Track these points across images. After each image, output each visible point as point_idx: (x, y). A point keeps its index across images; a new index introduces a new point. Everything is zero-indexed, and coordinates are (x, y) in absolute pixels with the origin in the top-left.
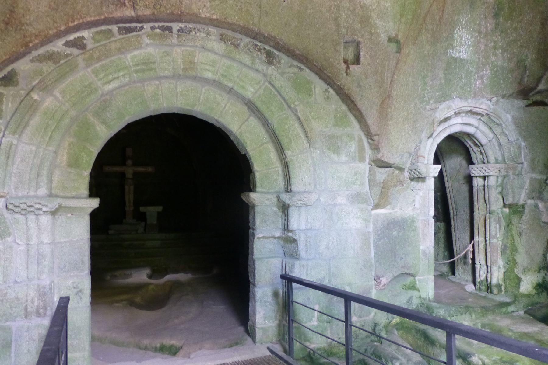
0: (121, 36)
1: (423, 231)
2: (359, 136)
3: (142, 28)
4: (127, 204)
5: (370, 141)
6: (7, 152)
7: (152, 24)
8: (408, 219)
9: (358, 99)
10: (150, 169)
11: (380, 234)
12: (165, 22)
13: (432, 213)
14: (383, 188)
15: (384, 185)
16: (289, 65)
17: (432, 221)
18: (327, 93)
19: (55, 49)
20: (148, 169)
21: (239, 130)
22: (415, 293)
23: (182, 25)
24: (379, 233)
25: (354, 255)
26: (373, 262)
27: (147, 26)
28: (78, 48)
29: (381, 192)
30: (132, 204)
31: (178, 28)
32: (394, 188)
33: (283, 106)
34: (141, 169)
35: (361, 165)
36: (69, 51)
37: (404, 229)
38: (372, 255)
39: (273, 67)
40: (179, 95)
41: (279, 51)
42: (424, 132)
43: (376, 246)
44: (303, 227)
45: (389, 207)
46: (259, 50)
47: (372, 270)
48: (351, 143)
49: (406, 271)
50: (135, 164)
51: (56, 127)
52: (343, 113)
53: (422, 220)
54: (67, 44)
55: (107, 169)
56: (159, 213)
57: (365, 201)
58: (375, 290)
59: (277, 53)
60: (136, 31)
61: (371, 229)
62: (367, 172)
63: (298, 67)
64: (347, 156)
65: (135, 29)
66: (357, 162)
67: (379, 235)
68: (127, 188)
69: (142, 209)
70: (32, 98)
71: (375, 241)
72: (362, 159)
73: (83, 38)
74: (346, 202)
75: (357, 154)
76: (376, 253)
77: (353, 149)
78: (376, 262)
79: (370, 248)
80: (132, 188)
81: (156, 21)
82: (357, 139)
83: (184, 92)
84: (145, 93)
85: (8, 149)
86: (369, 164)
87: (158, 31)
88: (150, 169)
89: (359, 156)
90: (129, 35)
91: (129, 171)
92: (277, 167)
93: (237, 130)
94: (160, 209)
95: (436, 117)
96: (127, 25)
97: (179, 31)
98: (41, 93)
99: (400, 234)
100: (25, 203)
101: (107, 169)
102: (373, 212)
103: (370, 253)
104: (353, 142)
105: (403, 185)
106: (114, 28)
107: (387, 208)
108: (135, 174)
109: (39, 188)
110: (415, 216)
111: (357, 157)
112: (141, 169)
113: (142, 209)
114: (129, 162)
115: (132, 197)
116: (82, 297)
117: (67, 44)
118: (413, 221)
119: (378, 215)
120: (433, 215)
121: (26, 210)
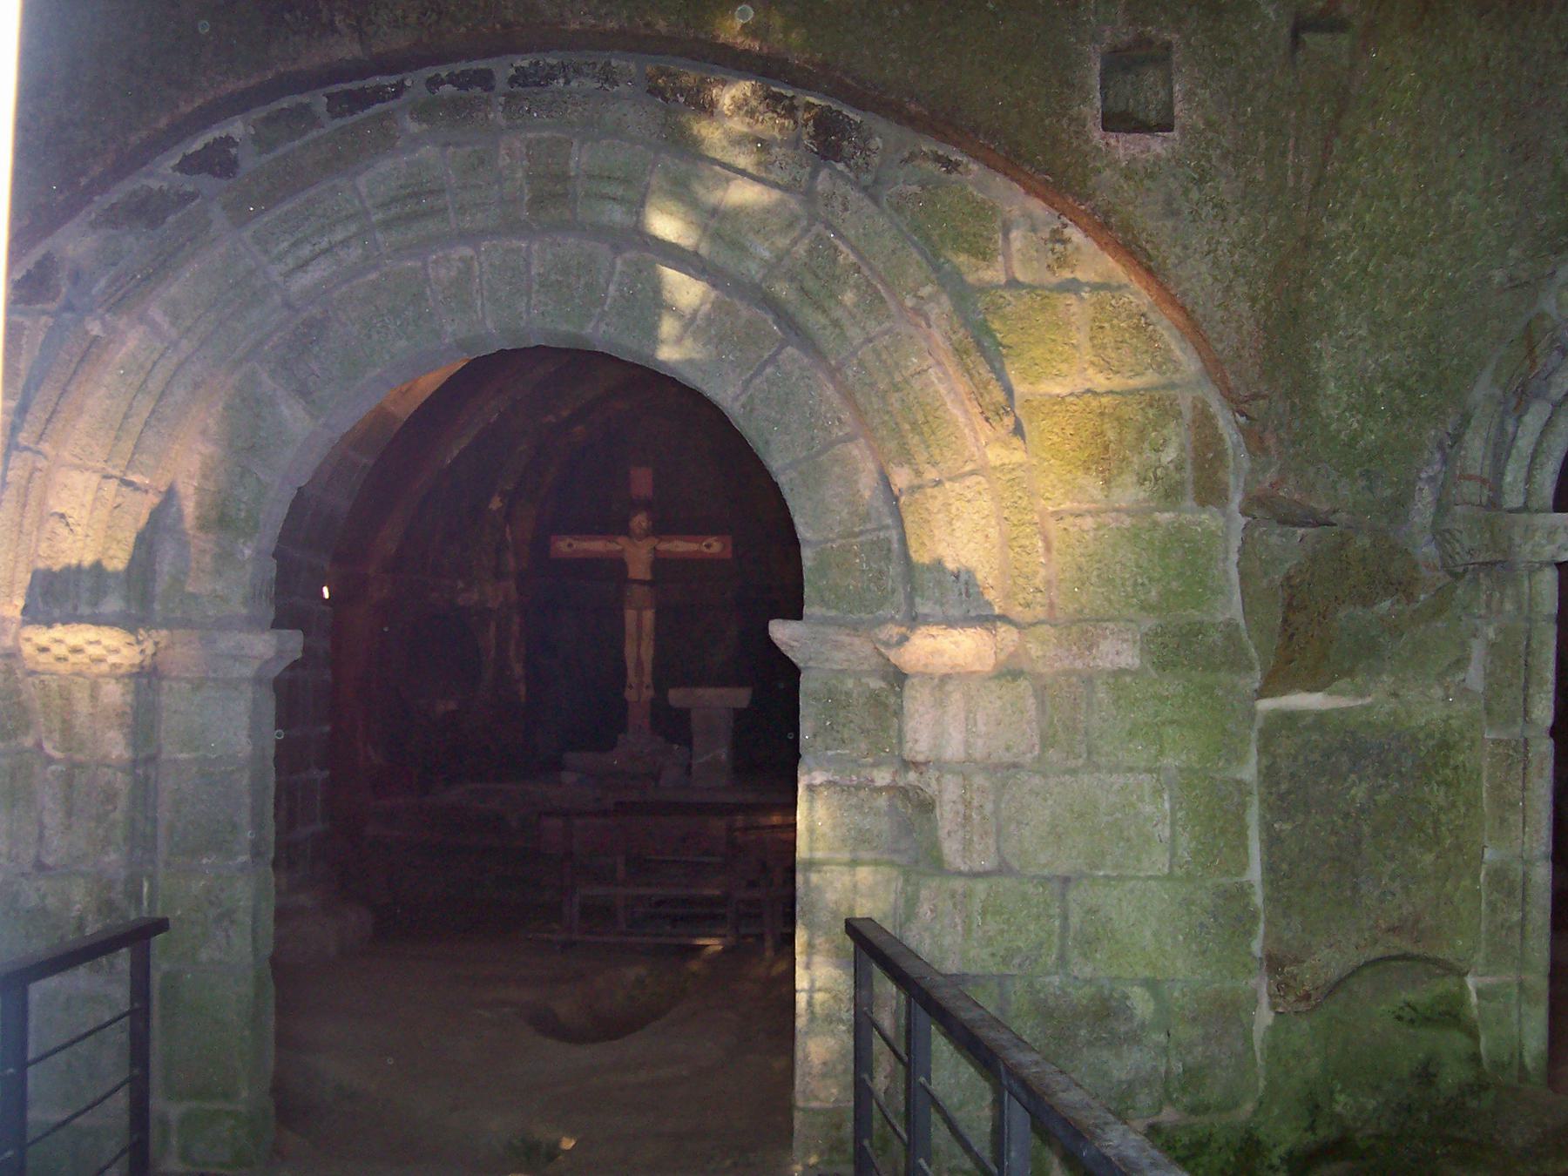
0: (339, 122)
1: (1500, 787)
2: (1200, 406)
3: (400, 88)
4: (632, 677)
5: (1242, 420)
6: (22, 491)
7: (428, 72)
8: (1421, 736)
9: (1172, 260)
10: (715, 546)
11: (1289, 792)
12: (469, 59)
13: (1544, 711)
14: (1290, 607)
15: (1292, 597)
16: (906, 154)
17: (1544, 747)
18: (1058, 247)
19: (155, 184)
20: (708, 546)
21: (743, 399)
22: (1459, 1041)
23: (523, 62)
24: (1284, 787)
25: (1171, 867)
26: (1258, 899)
27: (415, 81)
28: (215, 174)
29: (1285, 621)
30: (647, 679)
31: (512, 71)
32: (1359, 608)
33: (882, 301)
34: (681, 546)
35: (1204, 516)
36: (189, 184)
37: (1400, 772)
38: (1255, 873)
39: (840, 166)
40: (536, 287)
41: (860, 106)
42: (1486, 378)
43: (1272, 841)
44: (953, 749)
45: (1343, 683)
46: (791, 111)
47: (1250, 934)
48: (1165, 432)
49: (1401, 944)
50: (663, 527)
51: (153, 412)
52: (1130, 317)
53: (1493, 741)
54: (189, 165)
55: (566, 546)
56: (738, 714)
57: (1235, 661)
58: (1273, 1014)
59: (856, 117)
60: (383, 101)
61: (1249, 771)
62: (1235, 543)
63: (938, 159)
64: (1142, 481)
65: (378, 95)
66: (1189, 503)
67: (1281, 797)
68: (630, 615)
69: (676, 697)
70: (87, 333)
71: (1264, 817)
72: (1210, 492)
73: (228, 141)
74: (1137, 661)
75: (1188, 474)
76: (1270, 868)
77: (1169, 455)
78: (1268, 899)
79: (1246, 848)
80: (649, 616)
81: (438, 60)
82: (1188, 415)
83: (553, 277)
84: (428, 292)
85: (23, 482)
86: (1244, 513)
87: (448, 90)
88: (715, 546)
89: (1195, 483)
90: (361, 115)
91: (638, 556)
92: (887, 527)
93: (736, 398)
94: (741, 697)
95: (1541, 316)
96: (354, 85)
97: (513, 81)
98: (108, 317)
99: (1382, 798)
100: (98, 642)
101: (566, 546)
102: (1265, 705)
103: (1243, 867)
104: (1171, 430)
105: (1410, 597)
106: (318, 101)
107: (1333, 687)
108: (660, 563)
109: (105, 593)
110: (1454, 723)
111: (1189, 488)
112: (681, 546)
113: (676, 697)
114: (640, 521)
115: (648, 653)
116: (231, 933)
117: (189, 165)
118: (1445, 745)
119: (1290, 719)
120: (1549, 722)
121: (65, 659)
